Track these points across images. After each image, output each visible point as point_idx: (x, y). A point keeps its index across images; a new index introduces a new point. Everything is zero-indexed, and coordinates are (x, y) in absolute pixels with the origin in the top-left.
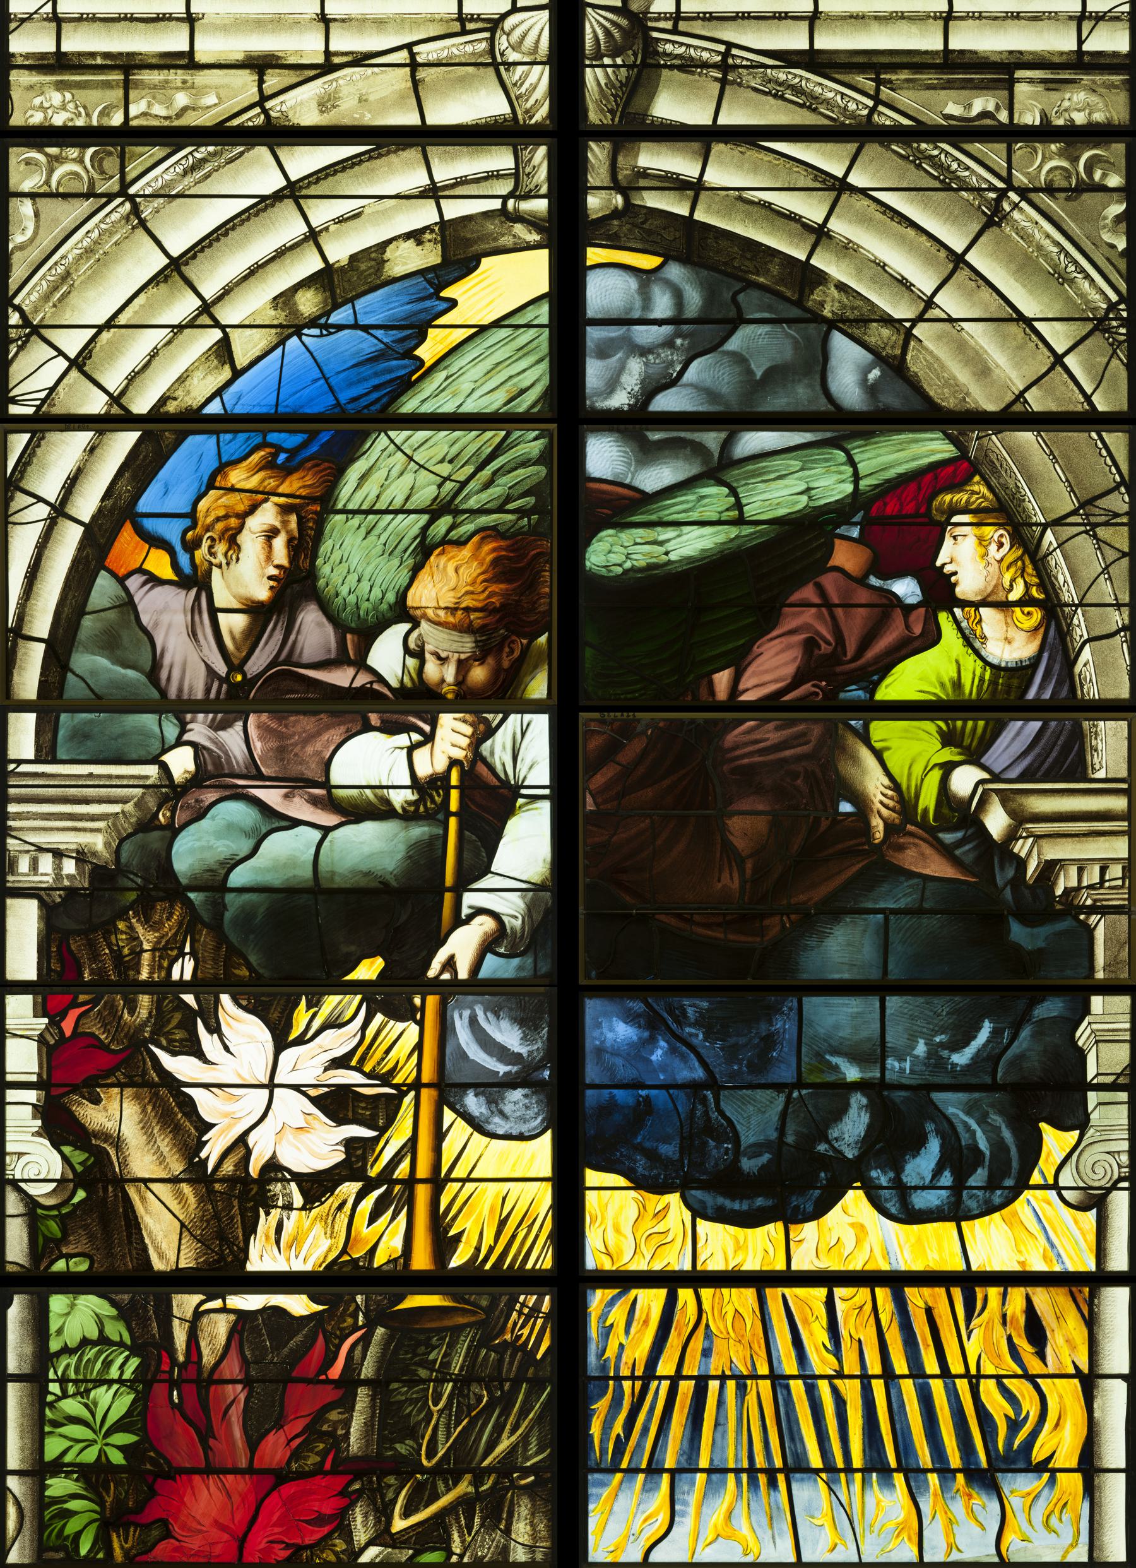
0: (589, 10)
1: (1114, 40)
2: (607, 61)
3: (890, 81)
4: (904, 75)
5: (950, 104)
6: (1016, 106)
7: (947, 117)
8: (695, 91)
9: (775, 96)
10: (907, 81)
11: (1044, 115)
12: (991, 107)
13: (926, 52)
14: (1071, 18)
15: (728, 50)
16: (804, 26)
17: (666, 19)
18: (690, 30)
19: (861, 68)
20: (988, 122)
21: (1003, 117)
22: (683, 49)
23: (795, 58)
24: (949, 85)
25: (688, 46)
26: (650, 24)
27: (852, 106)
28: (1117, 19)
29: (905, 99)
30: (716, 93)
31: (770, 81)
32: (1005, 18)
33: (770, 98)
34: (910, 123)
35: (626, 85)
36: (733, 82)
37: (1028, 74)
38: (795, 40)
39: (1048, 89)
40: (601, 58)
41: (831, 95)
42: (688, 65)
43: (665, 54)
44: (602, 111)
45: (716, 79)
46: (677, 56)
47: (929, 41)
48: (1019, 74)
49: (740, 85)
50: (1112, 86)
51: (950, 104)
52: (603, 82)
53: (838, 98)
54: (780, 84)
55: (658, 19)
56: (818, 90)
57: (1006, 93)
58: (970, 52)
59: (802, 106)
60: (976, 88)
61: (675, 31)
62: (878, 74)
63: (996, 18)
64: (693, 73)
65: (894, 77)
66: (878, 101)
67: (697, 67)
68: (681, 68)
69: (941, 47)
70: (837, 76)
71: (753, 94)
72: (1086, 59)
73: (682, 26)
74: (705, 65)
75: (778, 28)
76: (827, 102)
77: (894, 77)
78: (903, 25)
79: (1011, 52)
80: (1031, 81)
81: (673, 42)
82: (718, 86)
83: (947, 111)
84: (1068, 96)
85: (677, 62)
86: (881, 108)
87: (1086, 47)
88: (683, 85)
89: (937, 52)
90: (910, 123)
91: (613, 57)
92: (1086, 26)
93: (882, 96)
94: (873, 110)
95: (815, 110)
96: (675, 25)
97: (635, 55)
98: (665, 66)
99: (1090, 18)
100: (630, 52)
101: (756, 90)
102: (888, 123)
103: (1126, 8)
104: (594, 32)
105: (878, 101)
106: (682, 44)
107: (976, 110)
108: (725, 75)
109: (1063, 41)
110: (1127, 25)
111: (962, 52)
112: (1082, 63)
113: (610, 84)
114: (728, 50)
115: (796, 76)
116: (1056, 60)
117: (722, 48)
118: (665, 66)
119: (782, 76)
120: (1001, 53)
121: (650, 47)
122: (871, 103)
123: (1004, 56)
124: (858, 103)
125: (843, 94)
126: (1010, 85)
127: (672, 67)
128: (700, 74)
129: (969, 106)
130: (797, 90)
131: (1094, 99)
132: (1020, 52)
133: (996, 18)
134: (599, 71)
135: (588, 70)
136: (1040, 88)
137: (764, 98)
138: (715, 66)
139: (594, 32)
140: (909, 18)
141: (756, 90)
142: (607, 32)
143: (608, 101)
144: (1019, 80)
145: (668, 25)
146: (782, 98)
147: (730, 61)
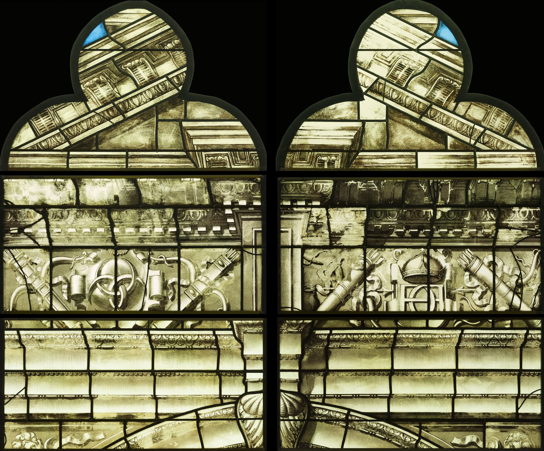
0: (282, 393)
1: (533, 408)
2: (291, 418)
3: (426, 428)
4: (433, 425)
5: (455, 438)
6: (487, 439)
7: (454, 445)
8: (333, 432)
9: (371, 435)
10: (434, 427)
11: (500, 444)
12: (474, 440)
13: (444, 414)
14: (513, 397)
15: (349, 413)
16: (385, 400)
17: (319, 398)
18: (330, 403)
19: (412, 421)
20: (473, 447)
21: (480, 444)
22: (327, 412)
23: (381, 416)
24: (454, 429)
25: (330, 411)
26: (311, 400)
27: (408, 439)
29: (433, 436)
30: (343, 433)
31: (369, 427)
32: (481, 397)
33: (369, 436)
34: (436, 447)
35: (300, 429)
36: (351, 428)
37: (493, 424)
38: (381, 408)
39: (502, 431)
40: (288, 416)
41: (398, 434)
42: (329, 420)
43: (319, 414)
44: (288, 442)
45: (343, 426)
46: (324, 416)
47: (445, 408)
48: (488, 424)
49: (354, 429)
50: (533, 430)
51: (455, 438)
52: (289, 428)
53: (402, 435)
54: (374, 429)
55: (315, 398)
56: (392, 432)
57: (482, 433)
58: (465, 413)
59: (384, 439)
60: (467, 431)
61: (323, 403)
62: (420, 424)
63: (477, 397)
64: (332, 424)
65: (428, 426)
66: (420, 437)
67: (334, 420)
68: (327, 421)
69: (451, 411)
70: (401, 425)
71: (361, 434)
72: (520, 417)
74: (338, 420)
75: (373, 402)
76: (396, 437)
77: (428, 426)
78: (433, 401)
79: (484, 414)
80: (494, 427)
81: (322, 409)
82: (344, 429)
83: (453, 442)
84: (511, 434)
85: (324, 418)
86: (422, 440)
87: (520, 411)
88: (327, 429)
89: (449, 414)
90: (436, 447)
92: (520, 401)
93: (423, 435)
94: (418, 441)
95: (390, 441)
96: (323, 401)
97: (304, 415)
98: (319, 420)
99: (522, 397)
100: (302, 414)
101: (362, 432)
102: (425, 447)
103: (539, 392)
104: (285, 404)
105: (420, 437)
106: (326, 410)
107: (467, 441)
108: (347, 424)
109: (509, 408)
110: (540, 400)
111: (460, 413)
112: (518, 419)
113: (292, 429)
114: (349, 413)
115: (381, 425)
116: (506, 417)
117: (346, 412)
118: (319, 420)
119: (374, 425)
120: (479, 414)
121: (311, 411)
122: (417, 438)
123: (481, 416)
124: (411, 438)
125: (404, 434)
126: (483, 429)
127: (322, 421)
128: (335, 424)
129: (464, 439)
130: (382, 432)
131: (524, 436)
132: (489, 414)
133: (477, 397)
134: (287, 422)
135: (282, 422)
136: (498, 431)
137: (366, 435)
138: (342, 420)
139: (285, 404)
140: (436, 397)
141: (362, 432)
142: (291, 404)
143: (291, 437)
144: (488, 427)
145: (320, 400)
146: (375, 435)
147: (350, 418)
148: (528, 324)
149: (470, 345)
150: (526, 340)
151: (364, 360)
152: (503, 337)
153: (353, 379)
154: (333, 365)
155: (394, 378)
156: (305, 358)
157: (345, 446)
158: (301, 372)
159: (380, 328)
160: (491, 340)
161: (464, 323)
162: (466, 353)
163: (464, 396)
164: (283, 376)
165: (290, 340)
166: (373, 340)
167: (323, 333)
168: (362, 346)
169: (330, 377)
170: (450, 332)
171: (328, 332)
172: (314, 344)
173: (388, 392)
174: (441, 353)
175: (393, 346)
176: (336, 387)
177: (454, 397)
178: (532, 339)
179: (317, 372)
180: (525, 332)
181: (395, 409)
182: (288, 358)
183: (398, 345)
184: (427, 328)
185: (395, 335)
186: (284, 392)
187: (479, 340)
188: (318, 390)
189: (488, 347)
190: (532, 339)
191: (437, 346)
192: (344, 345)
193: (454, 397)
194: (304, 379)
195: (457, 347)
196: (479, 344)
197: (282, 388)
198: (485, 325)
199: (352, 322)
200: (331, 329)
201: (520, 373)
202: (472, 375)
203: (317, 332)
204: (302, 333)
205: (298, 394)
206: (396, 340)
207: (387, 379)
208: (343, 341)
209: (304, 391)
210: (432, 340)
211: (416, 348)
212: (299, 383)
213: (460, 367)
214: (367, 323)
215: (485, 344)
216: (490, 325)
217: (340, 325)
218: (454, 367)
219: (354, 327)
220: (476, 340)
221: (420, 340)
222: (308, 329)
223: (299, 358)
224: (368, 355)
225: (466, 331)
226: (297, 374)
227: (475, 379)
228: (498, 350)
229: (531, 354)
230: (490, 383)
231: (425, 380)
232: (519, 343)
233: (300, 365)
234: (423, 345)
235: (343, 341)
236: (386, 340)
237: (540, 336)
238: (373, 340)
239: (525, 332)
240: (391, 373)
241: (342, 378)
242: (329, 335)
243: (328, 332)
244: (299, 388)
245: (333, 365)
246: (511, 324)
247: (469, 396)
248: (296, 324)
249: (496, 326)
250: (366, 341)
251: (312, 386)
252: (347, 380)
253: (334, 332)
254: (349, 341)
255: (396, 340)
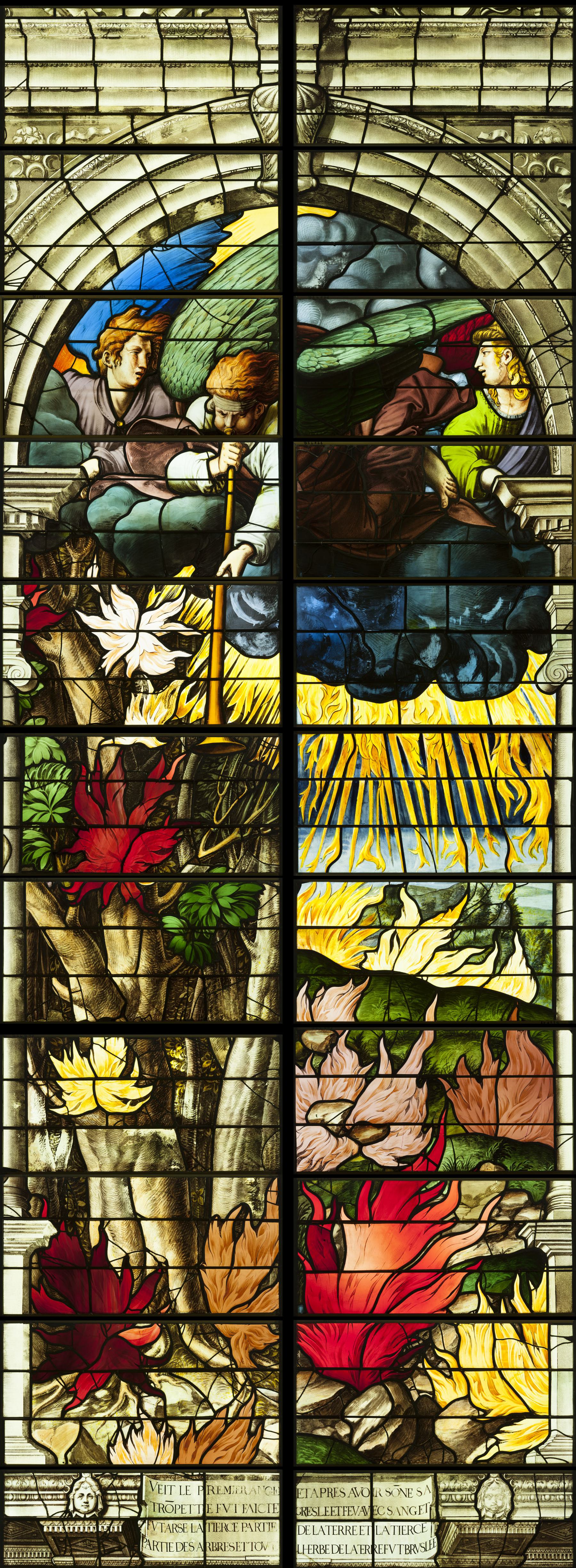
1: (565, 101)
2: (308, 111)
4: (458, 118)
8: (353, 126)
11: (529, 139)
12: (502, 135)
16: (408, 93)
19: (437, 115)
20: (501, 142)
24: (481, 124)
27: (432, 134)
28: (566, 90)
29: (459, 130)
37: (521, 118)
38: (403, 100)
42: (349, 113)
48: (517, 118)
50: (564, 124)
61: (342, 96)
66: (445, 131)
68: (346, 115)
73: (346, 93)
74: (358, 113)
76: (419, 132)
78: (458, 93)
80: (523, 121)
87: (551, 104)
88: (346, 123)
91: (311, 109)
92: (551, 93)
94: (442, 136)
103: (571, 84)
105: (445, 131)
107: (494, 137)
109: (539, 101)
112: (549, 112)
113: (309, 123)
116: (536, 110)
117: (366, 105)
119: (397, 119)
121: (330, 104)
126: (512, 123)
127: (341, 114)
129: (491, 134)
130: (404, 126)
131: (555, 130)
136: (527, 125)
138: (362, 114)
142: (308, 97)
145: (339, 93)
146: (397, 130)
148: (559, 12)
149: (498, 34)
150: (557, 29)
151: (385, 50)
152: (533, 25)
153: (374, 71)
154: (352, 55)
155: (417, 69)
156: (323, 48)
157: (366, 142)
158: (319, 63)
159: (403, 16)
160: (520, 29)
161: (491, 11)
162: (494, 42)
163: (491, 88)
164: (300, 67)
165: (307, 28)
166: (395, 29)
167: (341, 22)
168: (384, 35)
169: (349, 68)
170: (477, 20)
171: (347, 20)
172: (333, 33)
173: (411, 84)
174: (467, 43)
175: (416, 35)
176: (356, 79)
177: (481, 89)
178: (563, 28)
179: (336, 62)
180: (556, 20)
181: (417, 102)
182: (305, 48)
183: (421, 34)
184: (452, 16)
185: (419, 23)
186: (301, 84)
187: (507, 29)
188: (336, 82)
189: (517, 36)
190: (563, 28)
191: (462, 36)
192: (364, 34)
193: (481, 89)
194: (322, 71)
195: (484, 37)
196: (507, 33)
197: (298, 80)
198: (513, 13)
199: (373, 9)
200: (350, 18)
201: (551, 64)
202: (500, 66)
203: (336, 21)
204: (320, 21)
205: (316, 86)
206: (419, 29)
207: (410, 70)
208: (363, 30)
209: (322, 83)
210: (458, 29)
211: (440, 38)
212: (317, 74)
213: (487, 58)
214: (389, 11)
215: (514, 33)
216: (519, 13)
217: (360, 14)
218: (481, 58)
219: (375, 16)
220: (503, 28)
221: (445, 29)
222: (326, 18)
223: (317, 48)
224: (390, 45)
225: (493, 20)
226: (314, 65)
227: (502, 70)
228: (527, 40)
229: (562, 44)
230: (519, 75)
231: (450, 71)
232: (549, 32)
233: (318, 55)
234: (448, 34)
235: (363, 30)
236: (409, 29)
237: (571, 25)
238: (395, 29)
239: (556, 20)
240: (414, 64)
241: (361, 69)
242: (348, 24)
243: (347, 20)
244: (317, 80)
245: (352, 55)
246: (541, 12)
247: (496, 89)
248: (314, 12)
249: (525, 13)
250: (387, 30)
251: (330, 77)
252: (367, 72)
253: (353, 20)
254: (369, 29)
255: (419, 29)
